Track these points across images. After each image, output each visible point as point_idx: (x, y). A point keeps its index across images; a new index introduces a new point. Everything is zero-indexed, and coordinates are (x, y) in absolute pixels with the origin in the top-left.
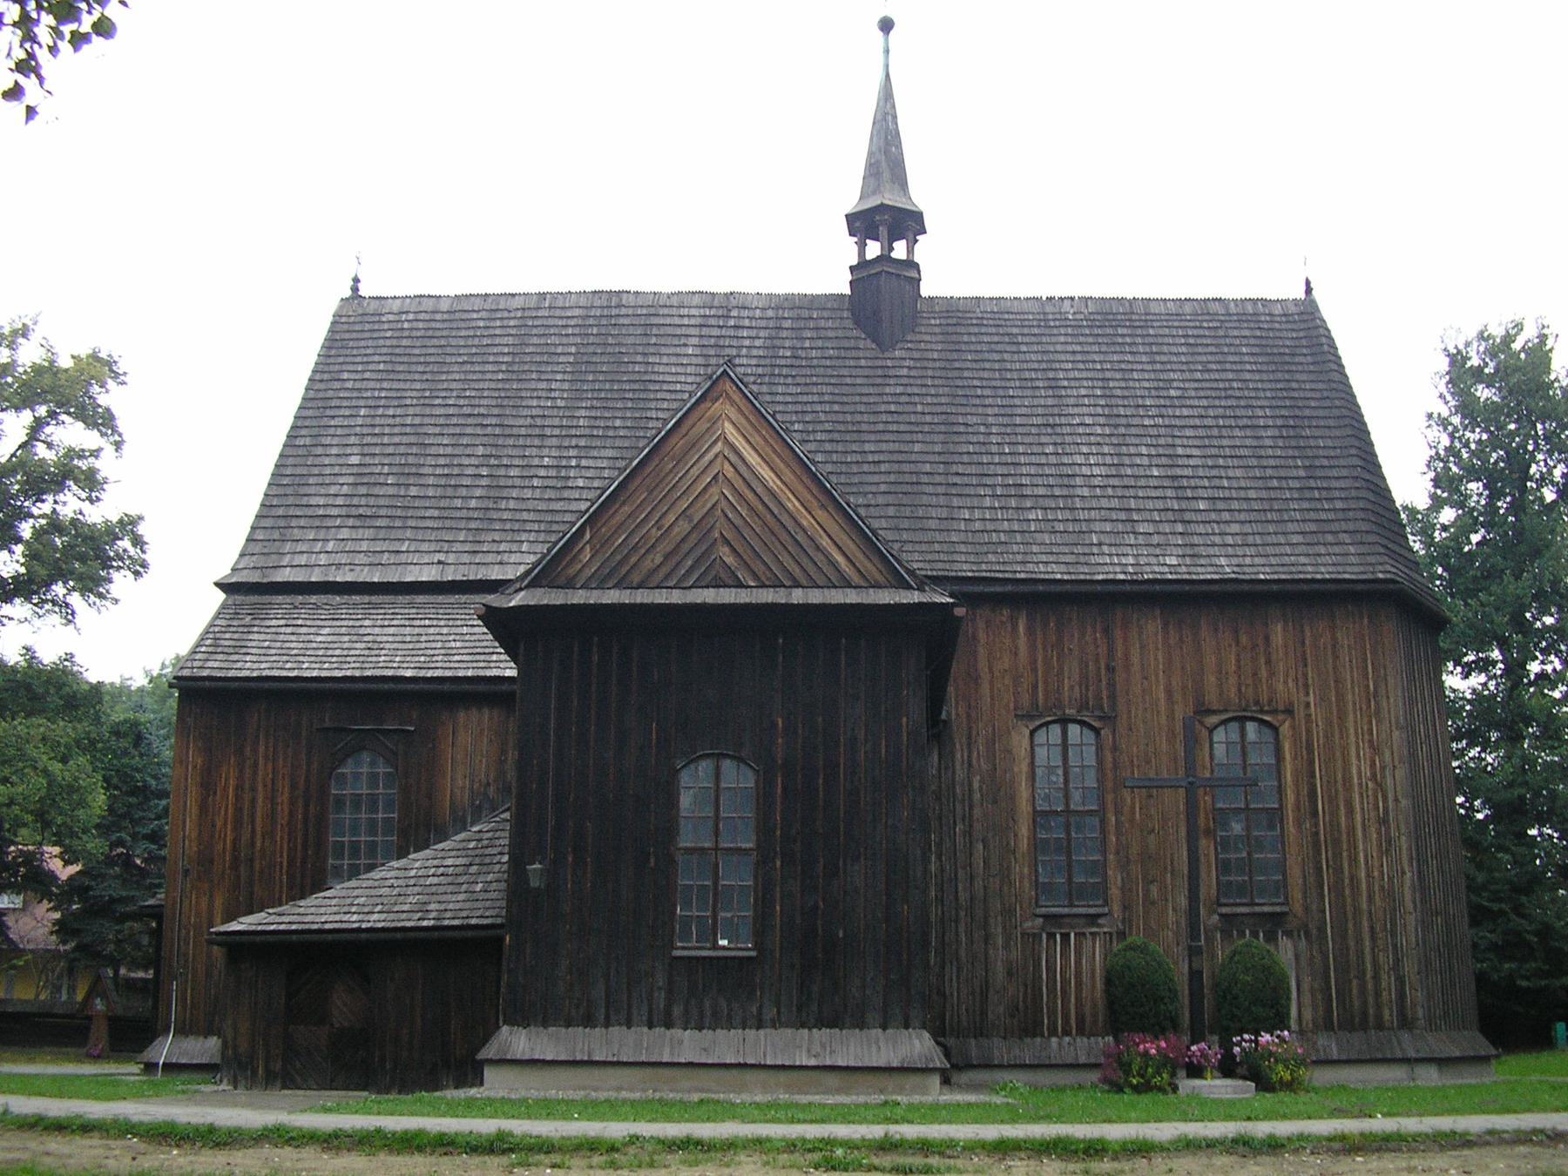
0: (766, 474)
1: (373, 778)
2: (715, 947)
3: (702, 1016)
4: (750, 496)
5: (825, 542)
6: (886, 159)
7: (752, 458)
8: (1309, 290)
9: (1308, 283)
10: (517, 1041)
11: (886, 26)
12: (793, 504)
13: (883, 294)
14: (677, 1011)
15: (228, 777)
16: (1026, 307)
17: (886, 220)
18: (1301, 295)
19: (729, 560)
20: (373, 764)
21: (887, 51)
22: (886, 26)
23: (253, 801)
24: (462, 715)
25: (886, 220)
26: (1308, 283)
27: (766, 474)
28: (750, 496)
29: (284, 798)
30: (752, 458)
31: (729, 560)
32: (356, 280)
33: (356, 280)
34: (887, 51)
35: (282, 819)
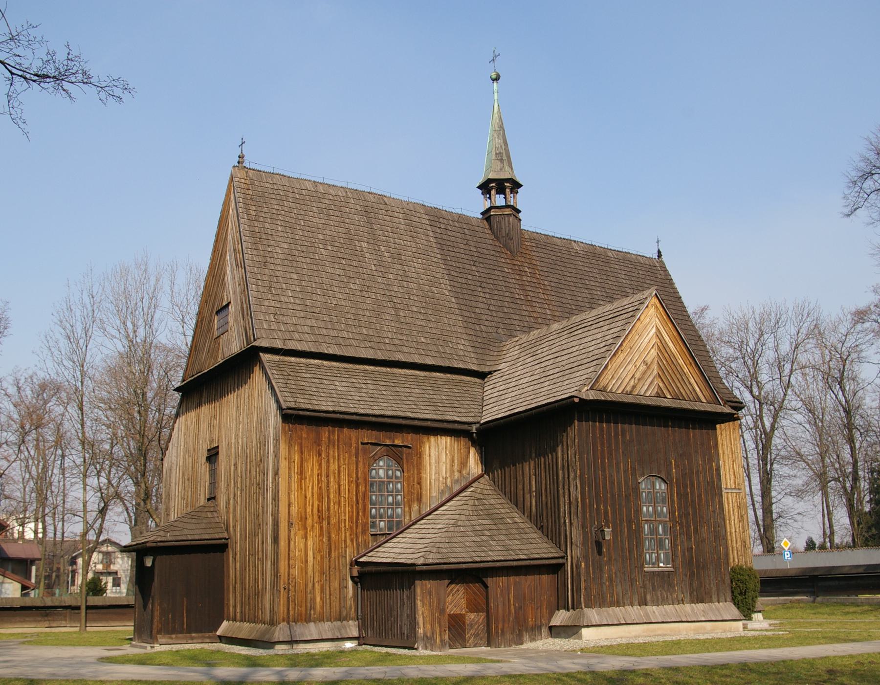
0: (671, 345)
2: (659, 567)
3: (658, 600)
4: (666, 355)
5: (692, 381)
7: (667, 339)
10: (592, 614)
12: (681, 361)
13: (500, 223)
14: (648, 597)
16: (558, 242)
18: (655, 256)
19: (661, 385)
23: (328, 483)
24: (432, 439)
27: (671, 345)
28: (666, 355)
29: (344, 481)
30: (667, 339)
31: (661, 385)
35: (345, 494)
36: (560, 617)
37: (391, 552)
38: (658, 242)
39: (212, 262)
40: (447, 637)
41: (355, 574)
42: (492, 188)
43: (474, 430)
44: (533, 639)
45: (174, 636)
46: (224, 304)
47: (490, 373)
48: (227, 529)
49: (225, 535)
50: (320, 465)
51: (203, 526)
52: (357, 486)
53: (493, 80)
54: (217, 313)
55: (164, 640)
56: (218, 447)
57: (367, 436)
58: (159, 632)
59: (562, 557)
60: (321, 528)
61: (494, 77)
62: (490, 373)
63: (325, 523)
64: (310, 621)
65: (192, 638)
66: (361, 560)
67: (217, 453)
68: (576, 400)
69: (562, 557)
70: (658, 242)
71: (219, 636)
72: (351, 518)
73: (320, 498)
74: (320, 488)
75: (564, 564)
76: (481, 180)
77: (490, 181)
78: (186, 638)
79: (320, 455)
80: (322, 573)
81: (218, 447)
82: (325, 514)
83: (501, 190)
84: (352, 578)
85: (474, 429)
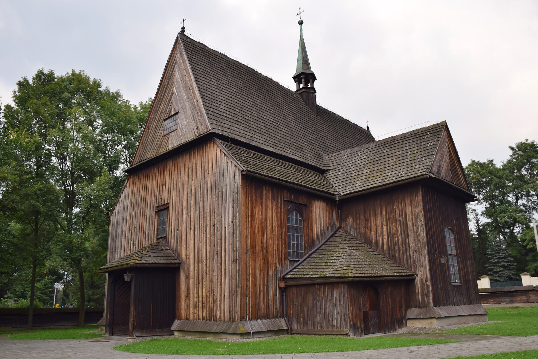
1: (297, 220)
6: (304, 60)
9: (368, 127)
11: (301, 23)
15: (257, 211)
17: (305, 77)
18: (366, 129)
20: (296, 216)
21: (301, 30)
22: (301, 23)
25: (305, 77)
26: (368, 127)
29: (275, 224)
32: (183, 28)
33: (183, 28)
34: (301, 30)
35: (275, 233)
37: (307, 271)
38: (367, 122)
39: (159, 89)
40: (363, 326)
44: (399, 328)
45: (144, 331)
46: (173, 113)
47: (327, 171)
49: (177, 261)
50: (262, 212)
51: (162, 255)
52: (281, 228)
55: (138, 334)
56: (168, 203)
57: (286, 195)
58: (134, 328)
59: (413, 275)
60: (263, 254)
63: (265, 251)
64: (258, 318)
66: (288, 276)
67: (168, 207)
68: (428, 176)
70: (367, 122)
72: (278, 248)
73: (262, 235)
74: (262, 227)
79: (262, 205)
80: (264, 285)
81: (168, 203)
82: (265, 245)
84: (280, 288)
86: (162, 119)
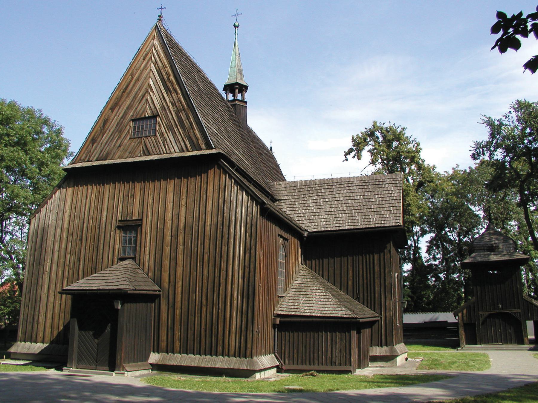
8: (271, 150)
9: (271, 148)
26: (271, 148)
36: (377, 351)
41: (278, 322)
42: (237, 88)
43: (306, 235)
47: (278, 200)
48: (159, 283)
53: (235, 26)
54: (134, 120)
56: (141, 220)
61: (237, 24)
62: (278, 200)
65: (140, 366)
67: (141, 225)
69: (379, 317)
71: (151, 364)
75: (378, 320)
76: (227, 82)
77: (237, 84)
78: (135, 366)
83: (241, 91)
85: (306, 234)
86: (129, 117)
